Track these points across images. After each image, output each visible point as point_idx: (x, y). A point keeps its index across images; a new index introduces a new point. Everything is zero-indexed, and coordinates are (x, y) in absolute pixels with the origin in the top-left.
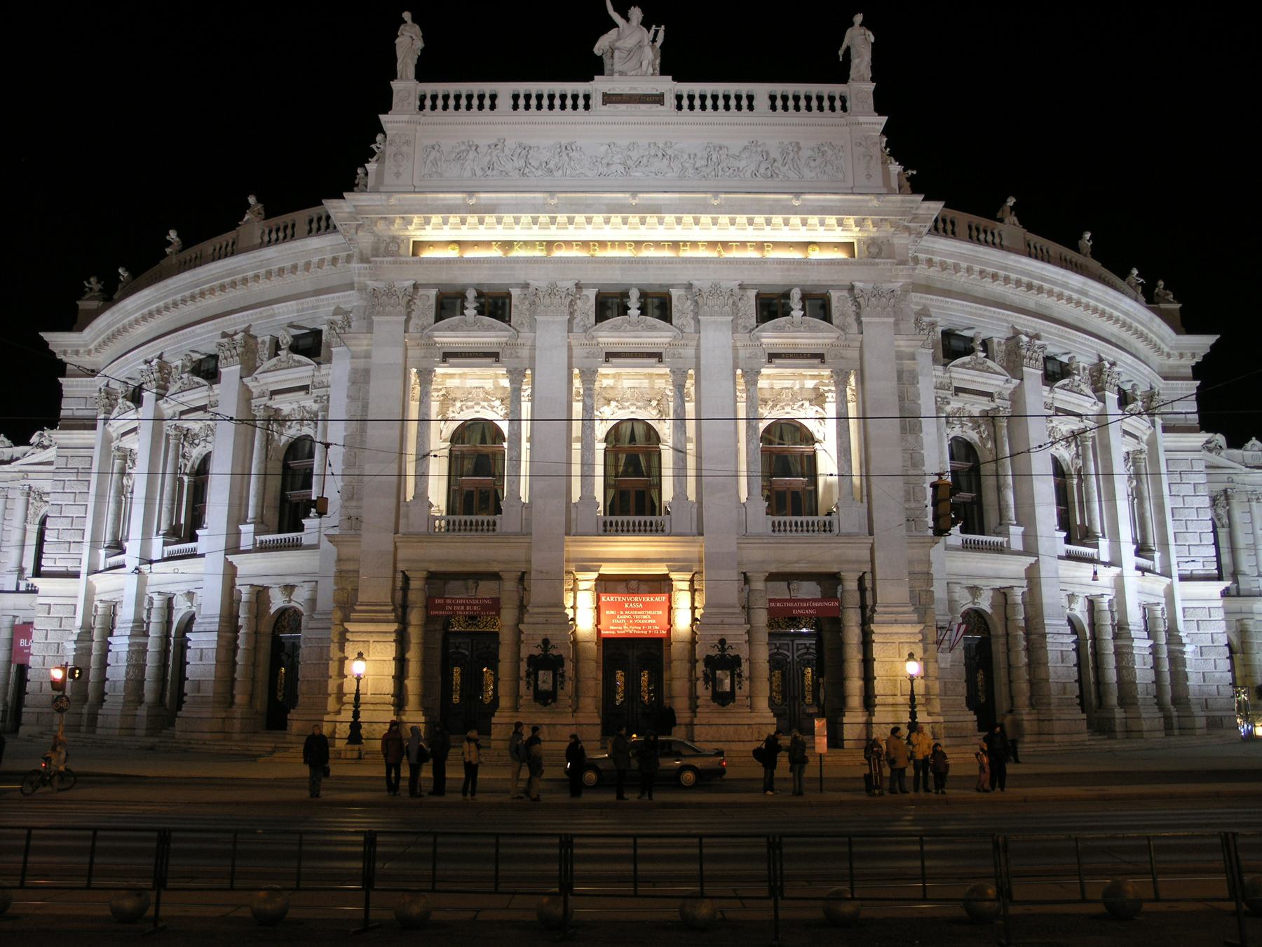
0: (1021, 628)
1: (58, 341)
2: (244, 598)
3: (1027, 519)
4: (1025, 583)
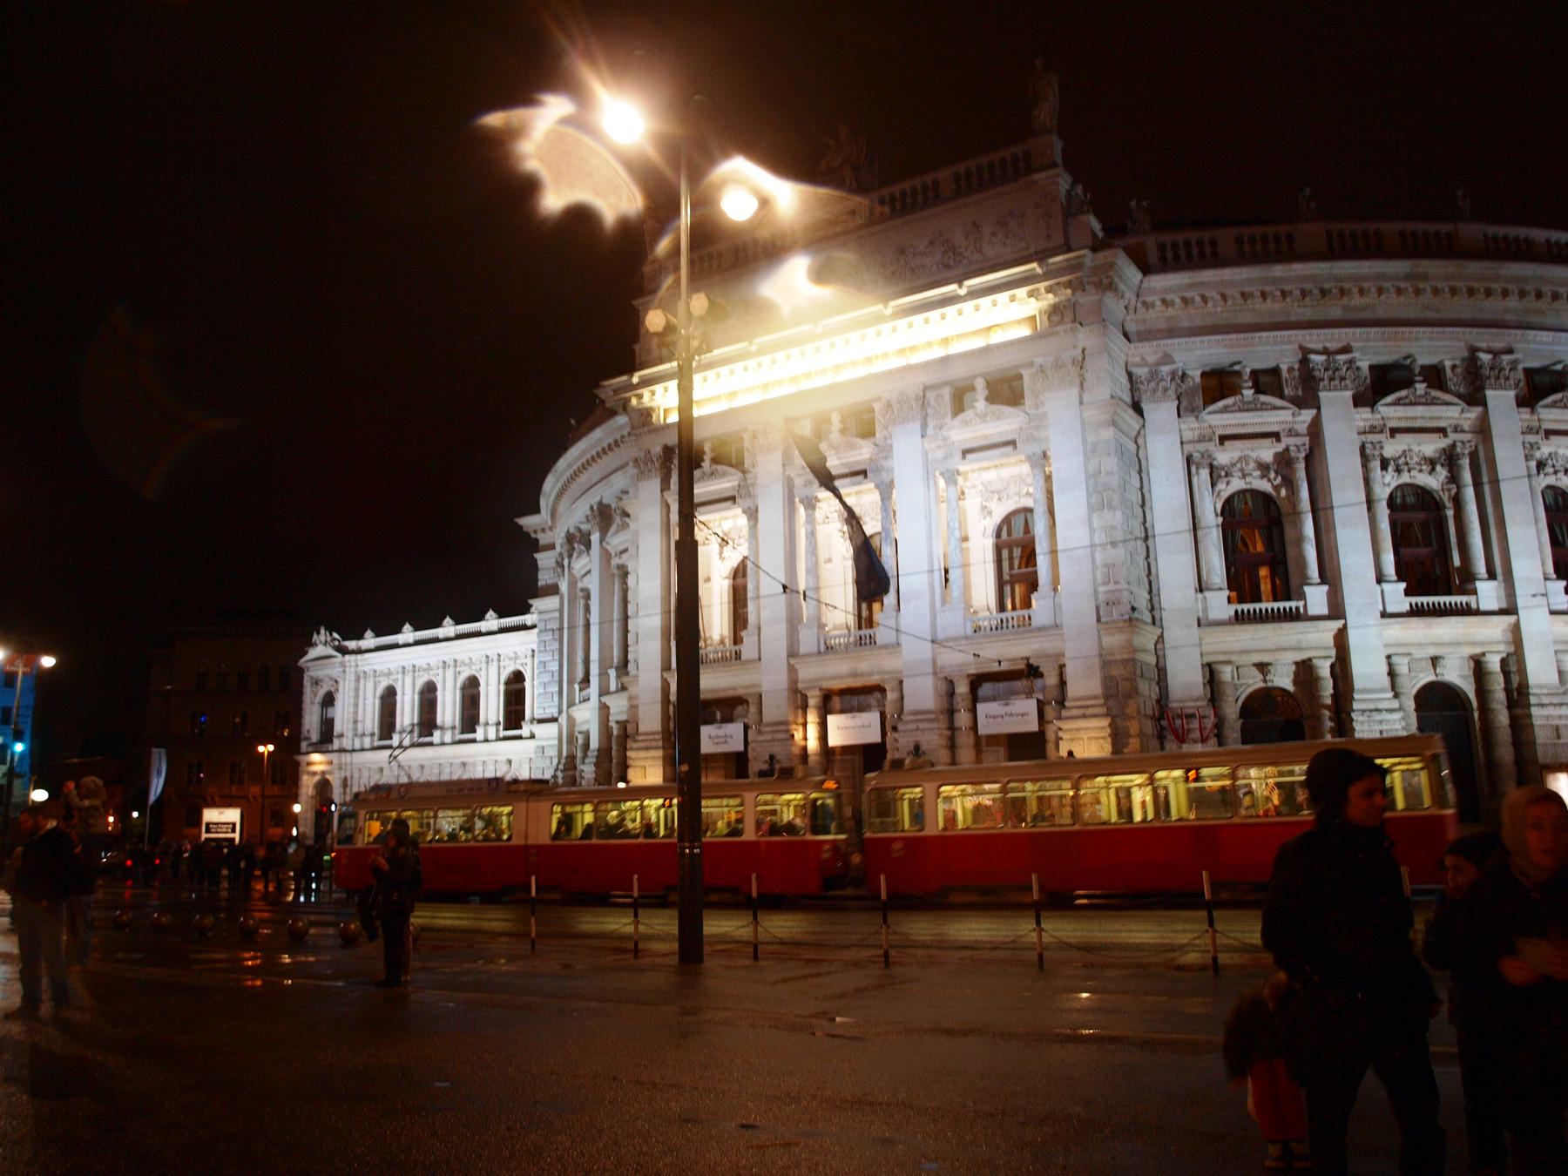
0: (1327, 707)
1: (528, 522)
2: (615, 732)
3: (1330, 575)
4: (1333, 652)
